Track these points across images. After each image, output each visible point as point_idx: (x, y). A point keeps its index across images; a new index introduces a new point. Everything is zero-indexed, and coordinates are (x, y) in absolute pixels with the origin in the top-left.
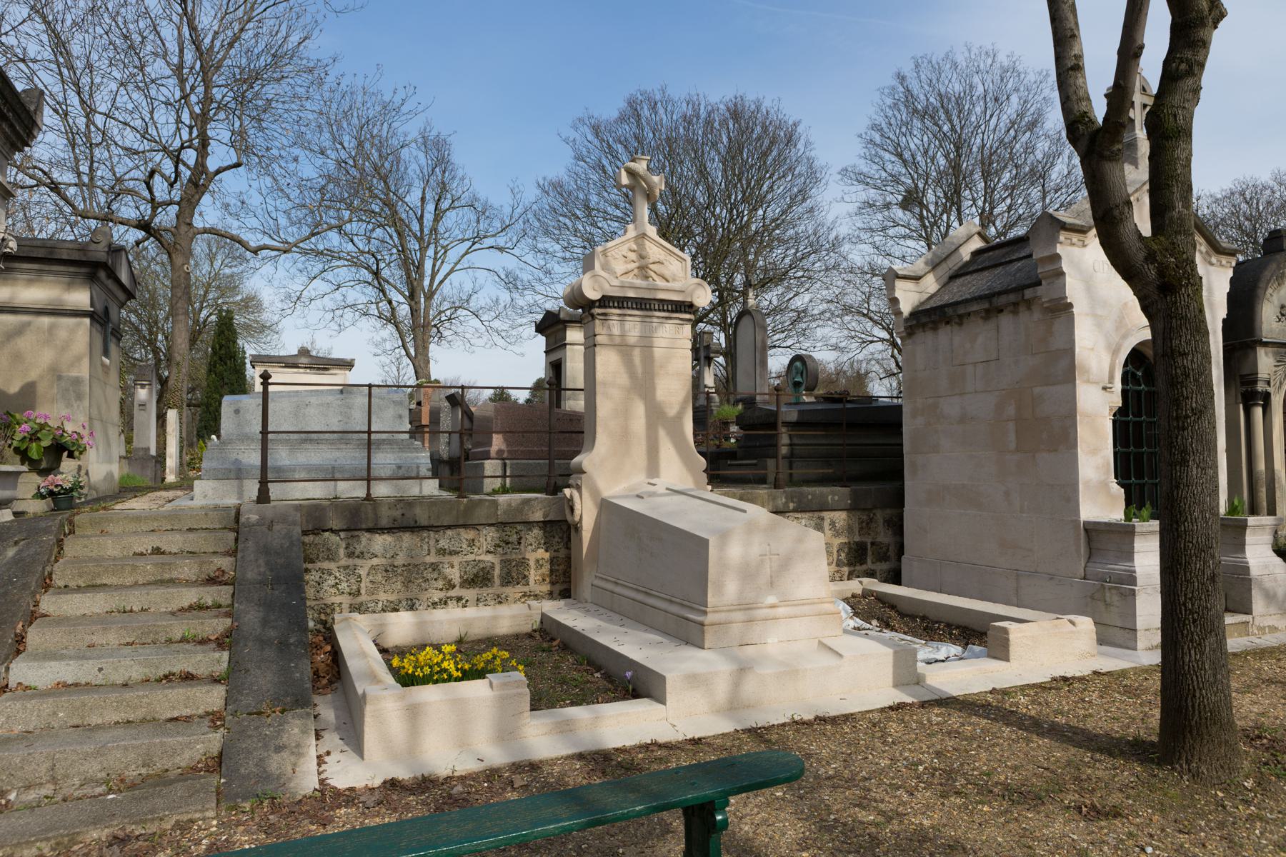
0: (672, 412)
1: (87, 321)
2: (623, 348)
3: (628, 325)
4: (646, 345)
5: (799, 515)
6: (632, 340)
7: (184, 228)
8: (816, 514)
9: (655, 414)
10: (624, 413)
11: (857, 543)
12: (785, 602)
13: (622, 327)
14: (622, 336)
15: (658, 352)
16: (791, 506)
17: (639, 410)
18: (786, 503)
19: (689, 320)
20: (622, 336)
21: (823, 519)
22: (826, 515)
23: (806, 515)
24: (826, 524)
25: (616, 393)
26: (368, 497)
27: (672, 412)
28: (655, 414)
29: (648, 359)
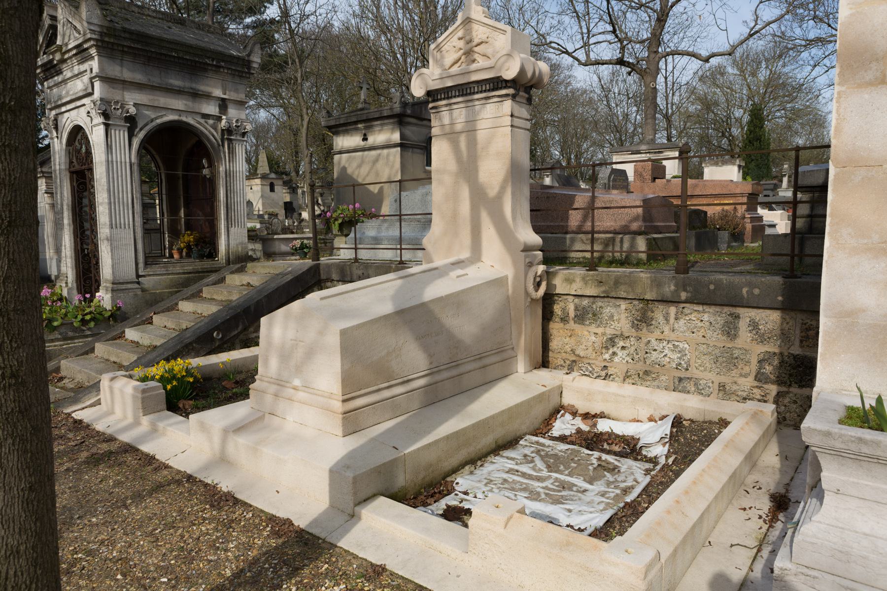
0: (492, 192)
1: (399, 149)
2: (452, 135)
3: (456, 113)
4: (471, 130)
5: (700, 308)
6: (459, 127)
7: (653, 55)
8: (727, 310)
9: (479, 196)
10: (455, 197)
11: (795, 357)
12: (306, 387)
13: (451, 115)
14: (452, 124)
15: (481, 135)
16: (684, 295)
17: (465, 193)
18: (676, 291)
19: (507, 95)
20: (452, 124)
21: (738, 317)
22: (747, 315)
23: (712, 309)
24: (743, 325)
25: (448, 180)
26: (356, 260)
27: (492, 192)
28: (479, 196)
29: (472, 143)
